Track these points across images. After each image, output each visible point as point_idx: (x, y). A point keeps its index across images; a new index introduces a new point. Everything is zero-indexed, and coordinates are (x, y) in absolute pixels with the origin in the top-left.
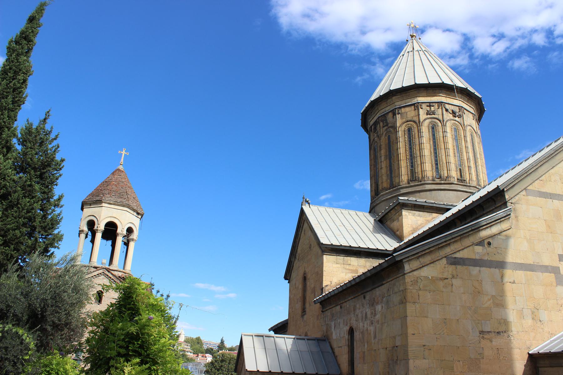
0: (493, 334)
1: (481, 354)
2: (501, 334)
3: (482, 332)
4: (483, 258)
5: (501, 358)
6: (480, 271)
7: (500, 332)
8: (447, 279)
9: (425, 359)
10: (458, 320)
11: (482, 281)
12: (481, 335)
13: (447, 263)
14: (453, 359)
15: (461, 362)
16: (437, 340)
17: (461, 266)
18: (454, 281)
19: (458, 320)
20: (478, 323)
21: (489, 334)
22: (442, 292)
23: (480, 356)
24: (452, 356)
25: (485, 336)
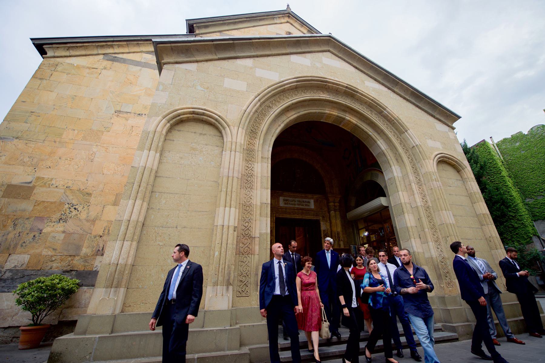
0: (133, 115)
1: (107, 127)
2: (143, 116)
3: (118, 112)
4: (149, 62)
5: (133, 134)
6: (141, 69)
7: (142, 114)
8: (97, 69)
9: (26, 123)
10: (92, 99)
11: (139, 77)
12: (116, 114)
13: (103, 59)
14: (67, 127)
15: (76, 132)
16: (53, 110)
17: (119, 63)
18: (104, 72)
19: (92, 99)
20: (117, 104)
21: (127, 114)
22: (84, 76)
23: (105, 129)
24: (66, 125)
25: (120, 115)
